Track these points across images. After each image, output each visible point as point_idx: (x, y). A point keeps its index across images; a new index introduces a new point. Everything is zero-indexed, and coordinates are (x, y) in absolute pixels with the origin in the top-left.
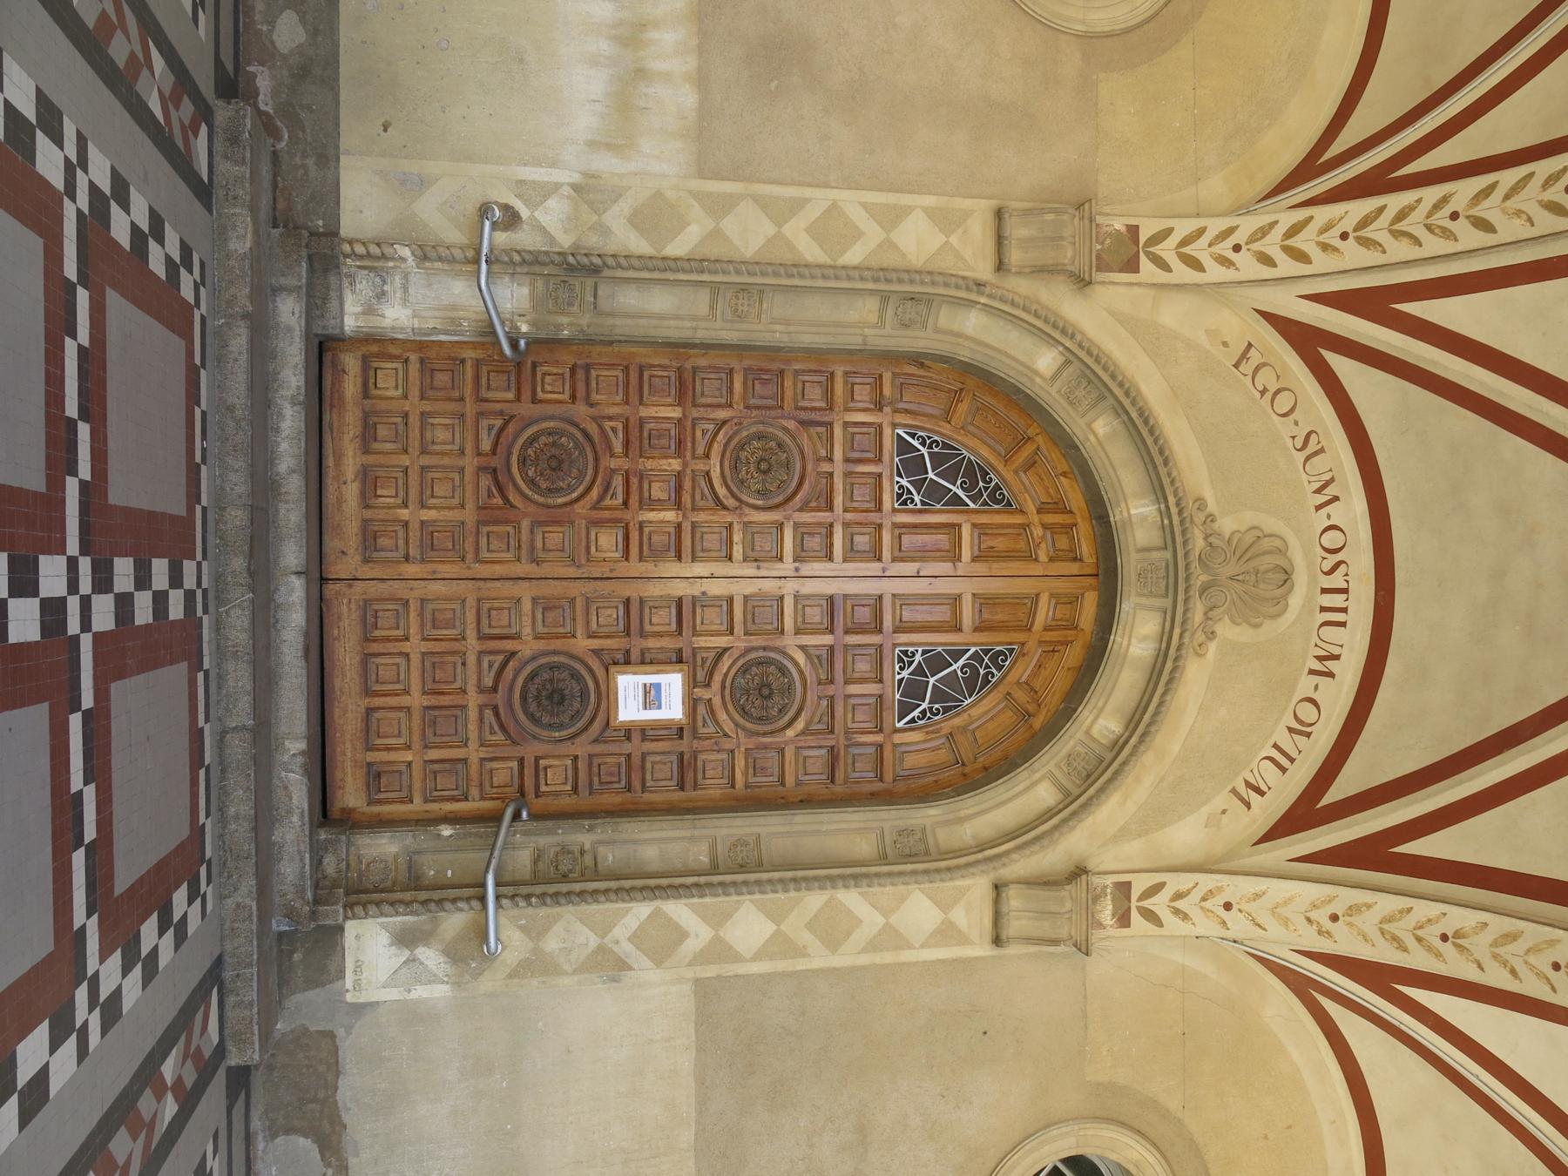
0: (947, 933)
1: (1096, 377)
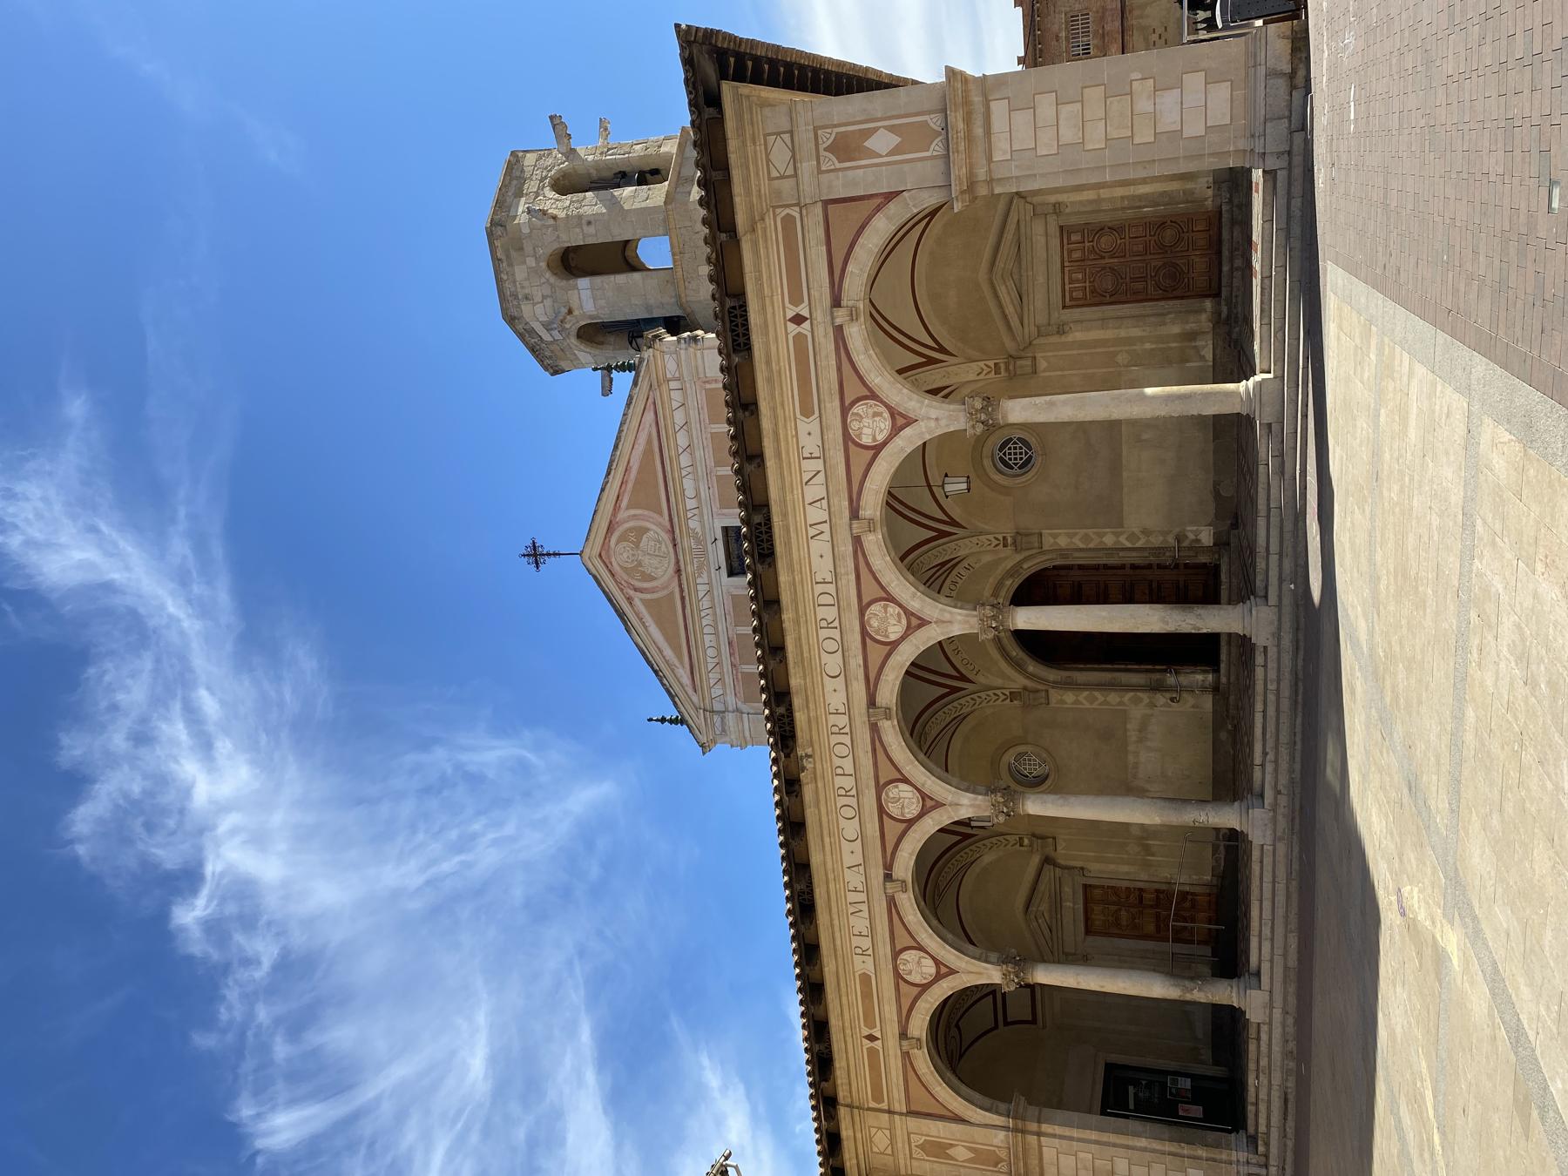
0: (1055, 536)
1: (1018, 666)
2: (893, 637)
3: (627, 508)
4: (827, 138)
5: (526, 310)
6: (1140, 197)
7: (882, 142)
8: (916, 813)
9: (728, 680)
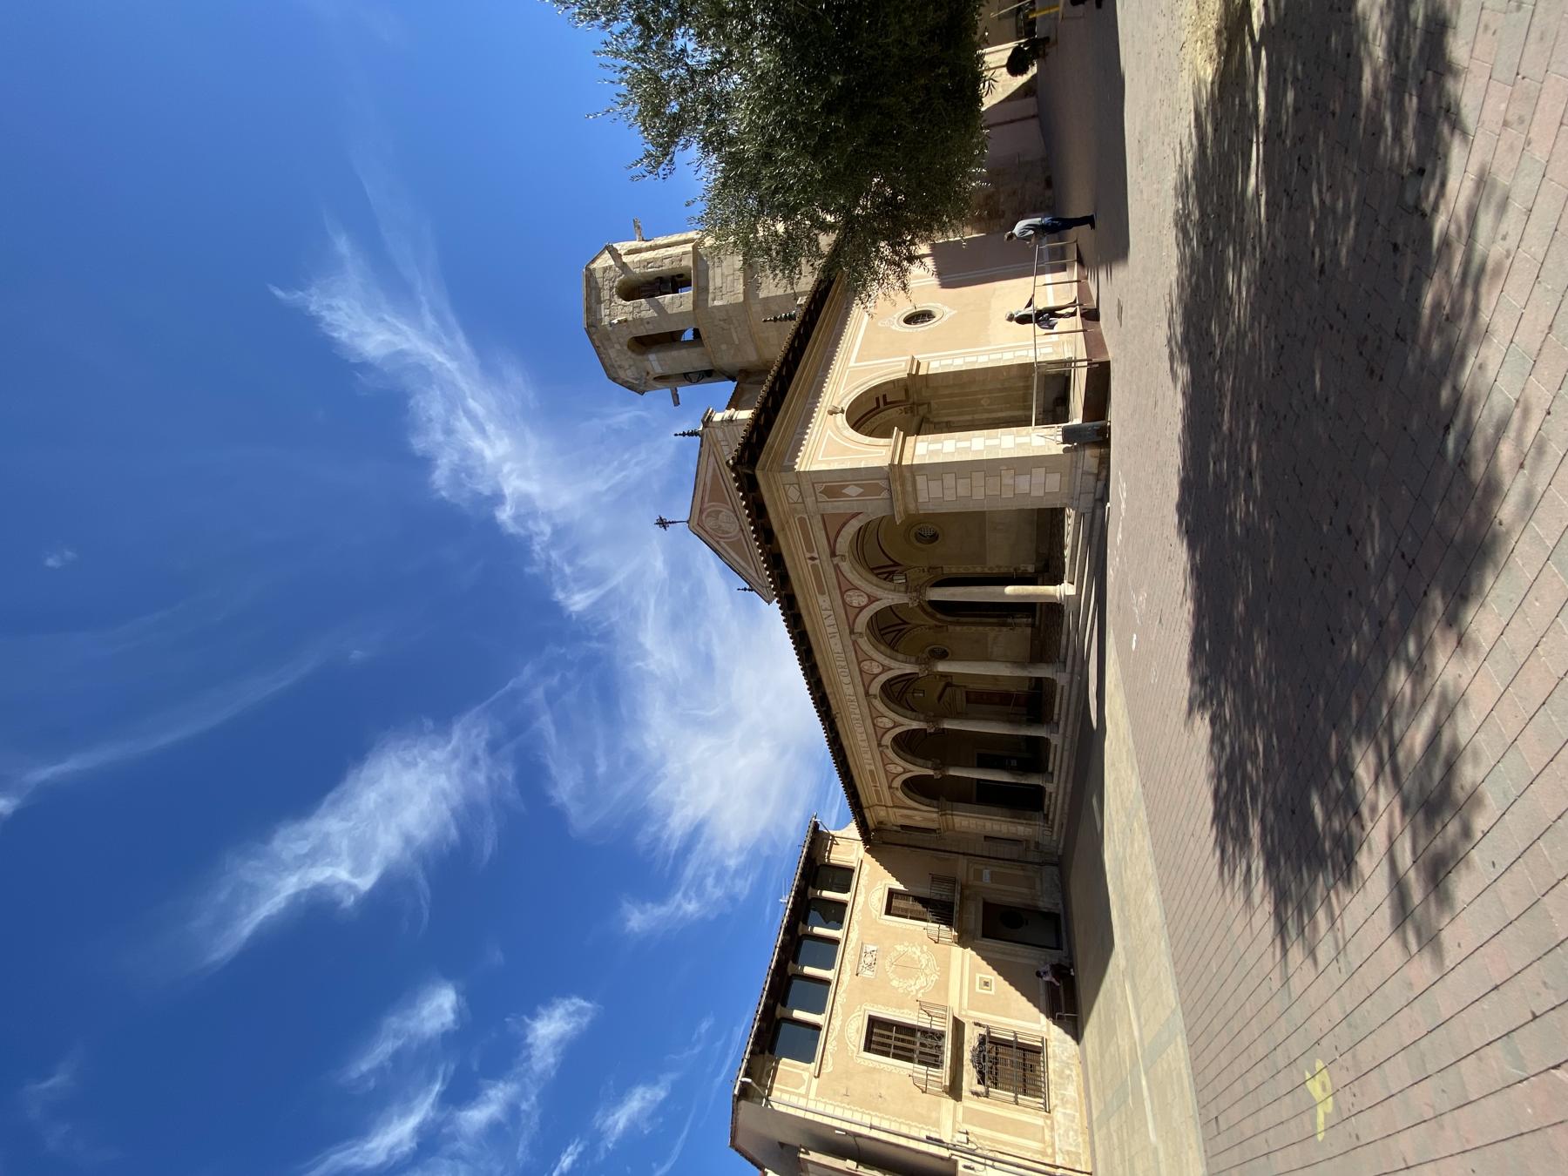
1: (932, 616)
4: (820, 488)
5: (622, 374)
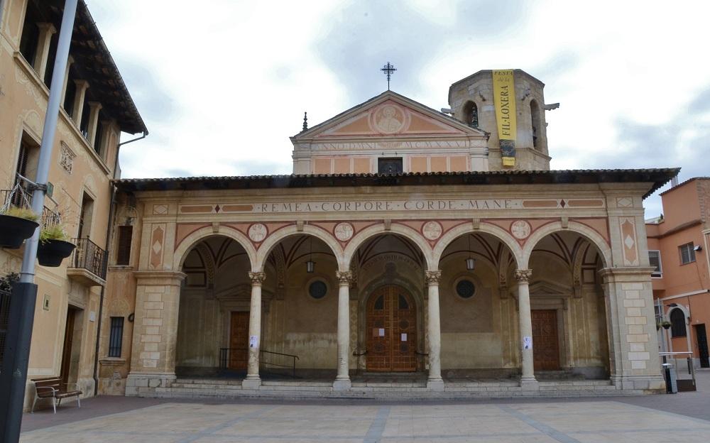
2: (424, 233)
3: (412, 116)
4: (631, 221)
6: (568, 340)
7: (629, 242)
8: (338, 238)
9: (327, 153)
